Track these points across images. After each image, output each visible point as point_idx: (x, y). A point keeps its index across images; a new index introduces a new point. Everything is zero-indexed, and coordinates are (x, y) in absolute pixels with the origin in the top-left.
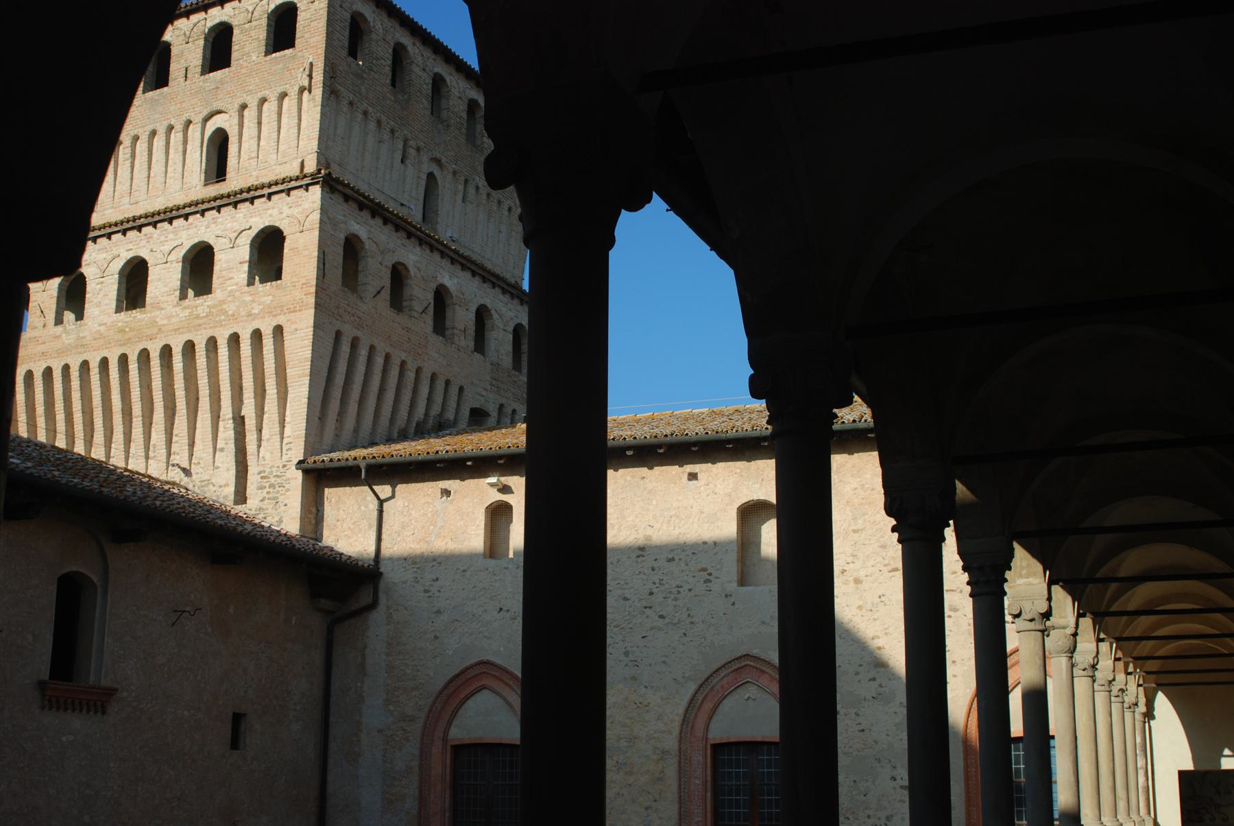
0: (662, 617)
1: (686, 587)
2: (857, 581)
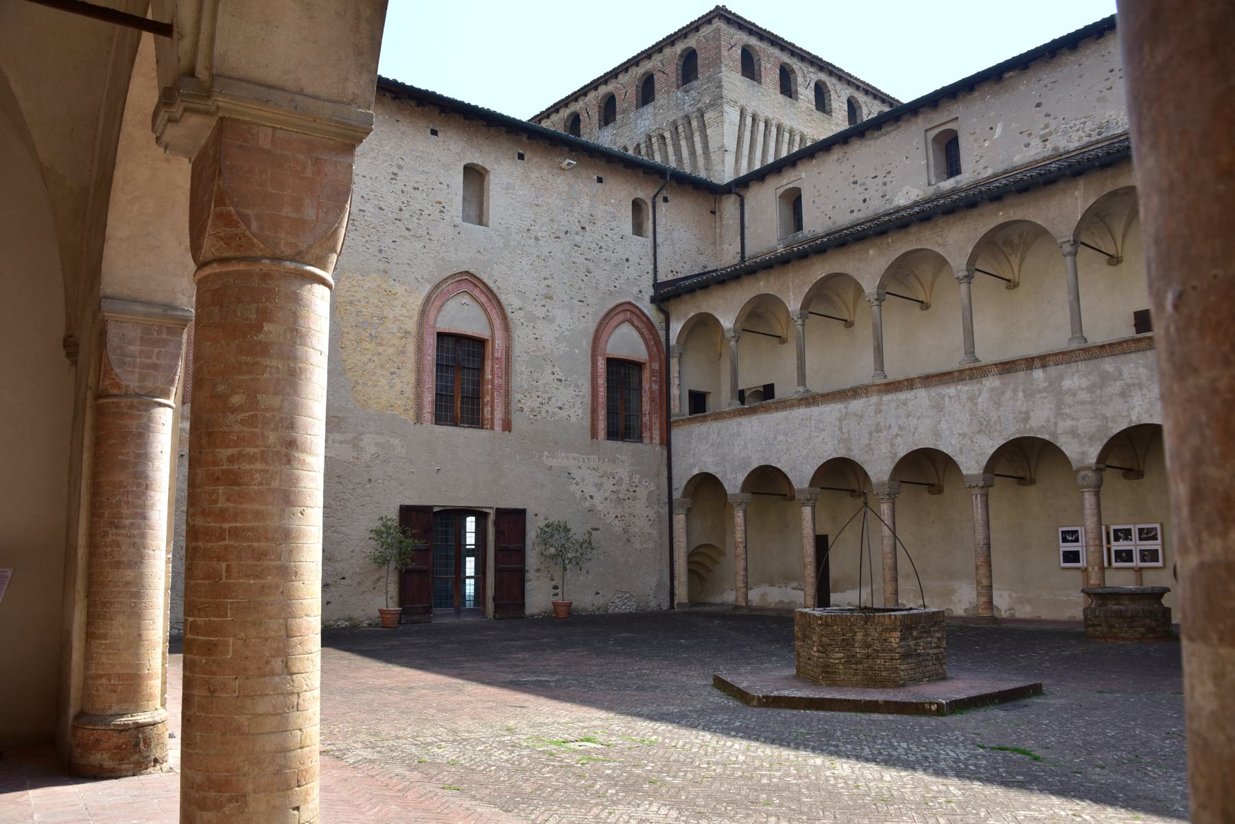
0: (408, 229)
1: (426, 212)
2: (537, 239)
